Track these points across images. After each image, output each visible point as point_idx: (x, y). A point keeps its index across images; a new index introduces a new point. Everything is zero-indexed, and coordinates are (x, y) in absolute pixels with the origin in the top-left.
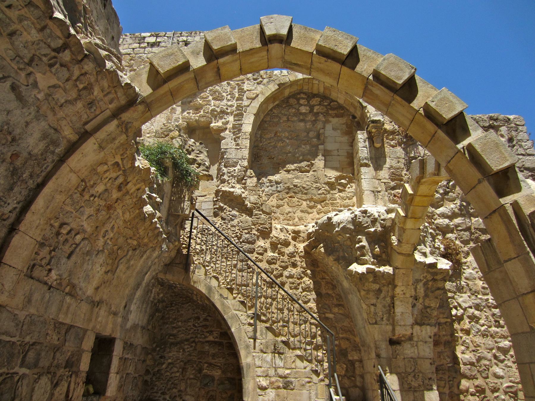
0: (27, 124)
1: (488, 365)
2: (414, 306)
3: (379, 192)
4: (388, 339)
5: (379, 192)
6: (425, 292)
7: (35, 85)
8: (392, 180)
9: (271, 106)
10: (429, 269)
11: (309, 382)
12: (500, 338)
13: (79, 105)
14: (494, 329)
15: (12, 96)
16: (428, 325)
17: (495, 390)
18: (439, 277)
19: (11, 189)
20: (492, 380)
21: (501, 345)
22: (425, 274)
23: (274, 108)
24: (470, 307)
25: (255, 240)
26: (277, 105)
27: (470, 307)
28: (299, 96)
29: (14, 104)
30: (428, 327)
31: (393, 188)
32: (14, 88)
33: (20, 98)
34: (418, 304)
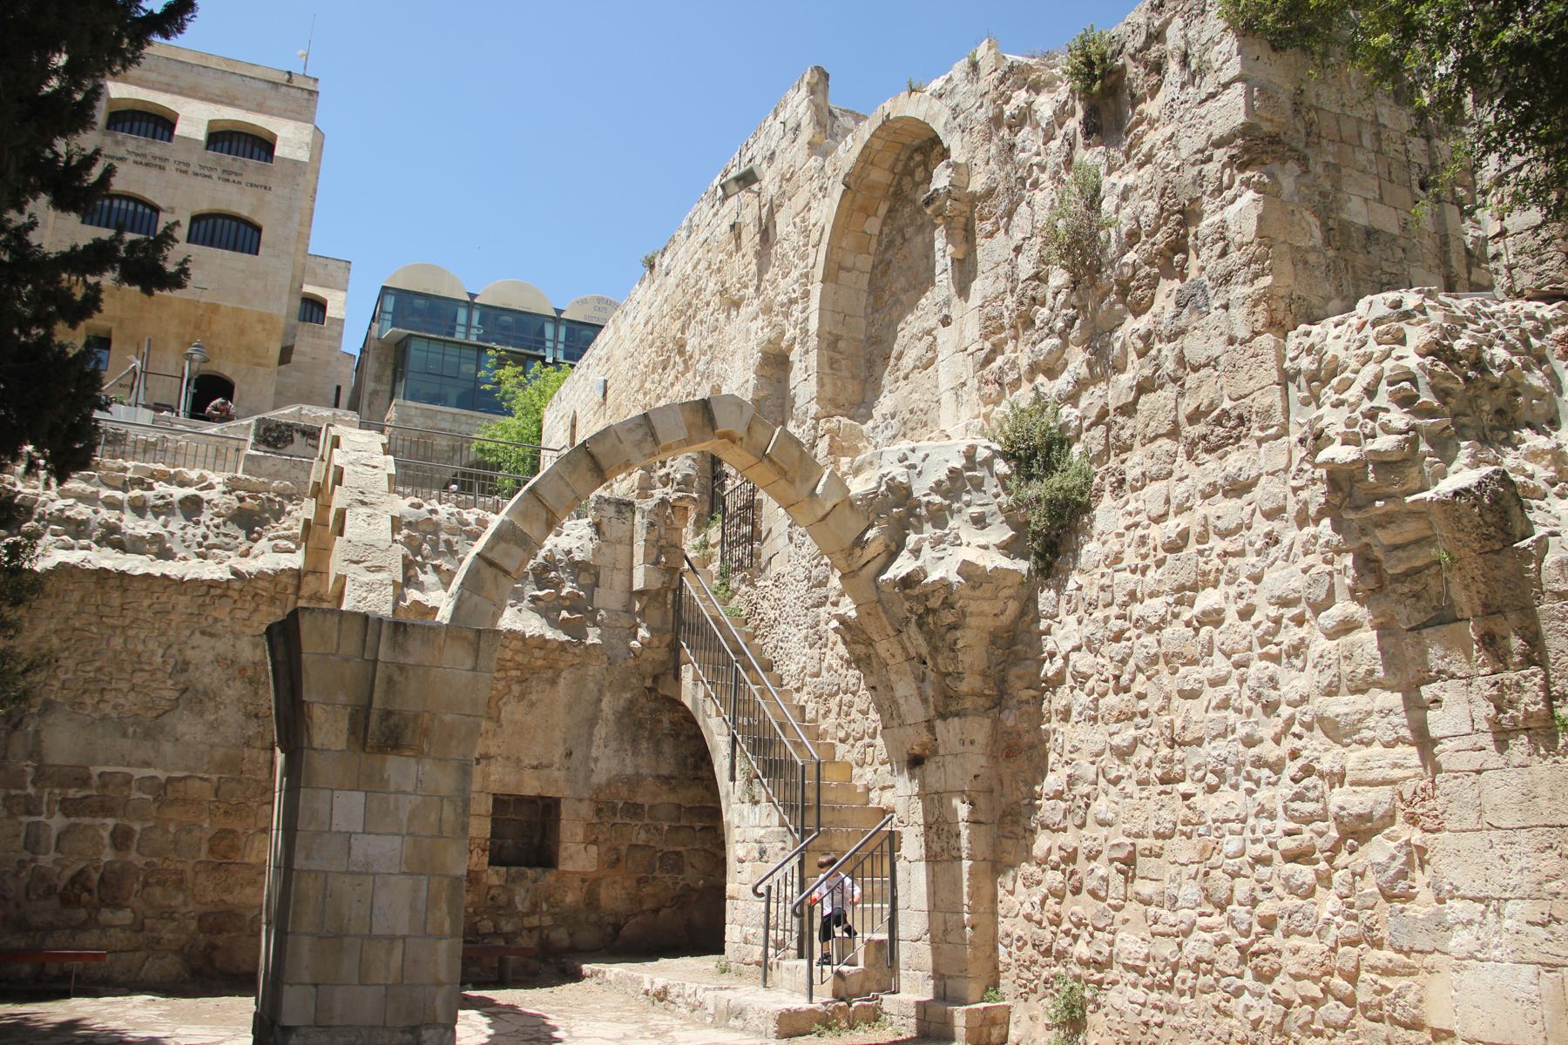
0: (233, 646)
1: (1088, 796)
2: (921, 679)
3: (964, 384)
4: (906, 757)
5: (964, 384)
6: (929, 643)
7: (216, 620)
8: (986, 337)
9: (873, 225)
10: (908, 591)
11: (783, 849)
12: (1118, 721)
13: (264, 608)
14: (1111, 699)
15: (206, 638)
16: (957, 714)
17: (1093, 856)
18: (934, 603)
19: (257, 693)
20: (1091, 830)
21: (1116, 740)
22: (907, 605)
23: (884, 224)
24: (1078, 649)
25: (827, 577)
26: (890, 211)
27: (1078, 649)
28: (912, 164)
29: (212, 642)
30: (956, 719)
31: (988, 361)
32: (203, 633)
33: (212, 635)
34: (928, 671)
